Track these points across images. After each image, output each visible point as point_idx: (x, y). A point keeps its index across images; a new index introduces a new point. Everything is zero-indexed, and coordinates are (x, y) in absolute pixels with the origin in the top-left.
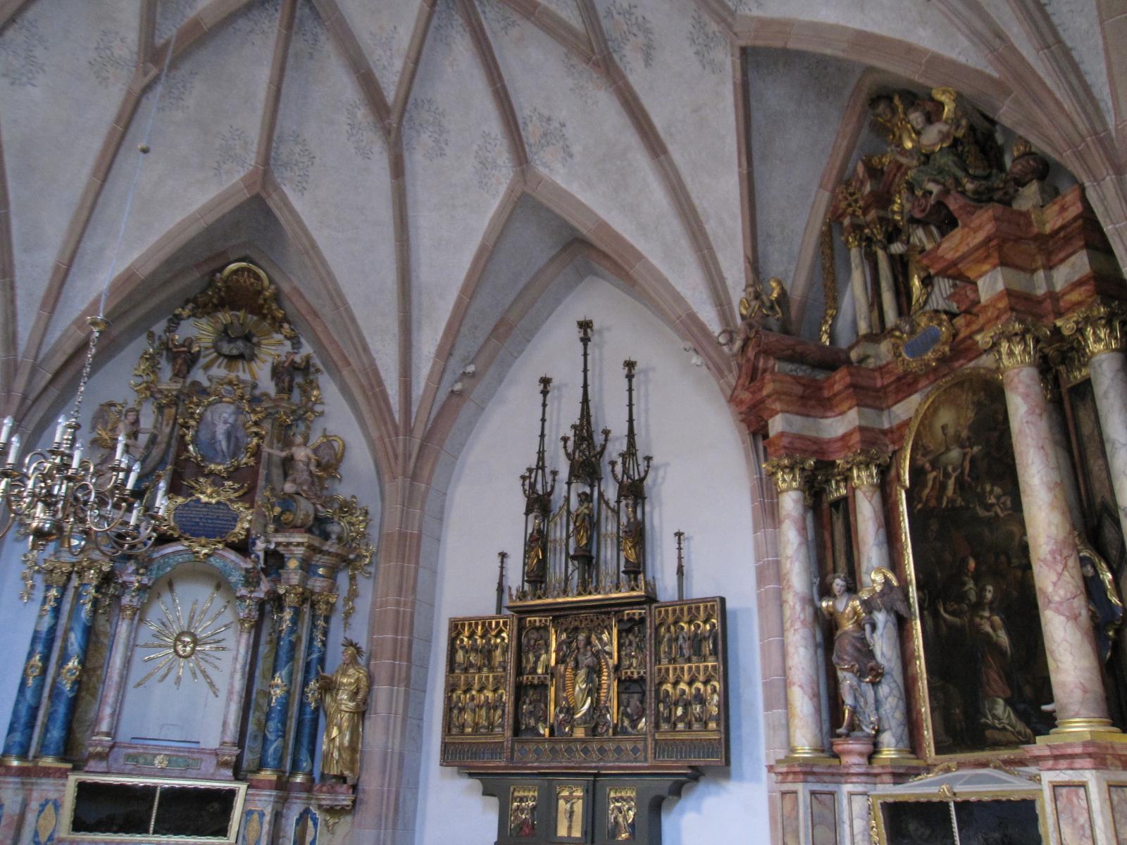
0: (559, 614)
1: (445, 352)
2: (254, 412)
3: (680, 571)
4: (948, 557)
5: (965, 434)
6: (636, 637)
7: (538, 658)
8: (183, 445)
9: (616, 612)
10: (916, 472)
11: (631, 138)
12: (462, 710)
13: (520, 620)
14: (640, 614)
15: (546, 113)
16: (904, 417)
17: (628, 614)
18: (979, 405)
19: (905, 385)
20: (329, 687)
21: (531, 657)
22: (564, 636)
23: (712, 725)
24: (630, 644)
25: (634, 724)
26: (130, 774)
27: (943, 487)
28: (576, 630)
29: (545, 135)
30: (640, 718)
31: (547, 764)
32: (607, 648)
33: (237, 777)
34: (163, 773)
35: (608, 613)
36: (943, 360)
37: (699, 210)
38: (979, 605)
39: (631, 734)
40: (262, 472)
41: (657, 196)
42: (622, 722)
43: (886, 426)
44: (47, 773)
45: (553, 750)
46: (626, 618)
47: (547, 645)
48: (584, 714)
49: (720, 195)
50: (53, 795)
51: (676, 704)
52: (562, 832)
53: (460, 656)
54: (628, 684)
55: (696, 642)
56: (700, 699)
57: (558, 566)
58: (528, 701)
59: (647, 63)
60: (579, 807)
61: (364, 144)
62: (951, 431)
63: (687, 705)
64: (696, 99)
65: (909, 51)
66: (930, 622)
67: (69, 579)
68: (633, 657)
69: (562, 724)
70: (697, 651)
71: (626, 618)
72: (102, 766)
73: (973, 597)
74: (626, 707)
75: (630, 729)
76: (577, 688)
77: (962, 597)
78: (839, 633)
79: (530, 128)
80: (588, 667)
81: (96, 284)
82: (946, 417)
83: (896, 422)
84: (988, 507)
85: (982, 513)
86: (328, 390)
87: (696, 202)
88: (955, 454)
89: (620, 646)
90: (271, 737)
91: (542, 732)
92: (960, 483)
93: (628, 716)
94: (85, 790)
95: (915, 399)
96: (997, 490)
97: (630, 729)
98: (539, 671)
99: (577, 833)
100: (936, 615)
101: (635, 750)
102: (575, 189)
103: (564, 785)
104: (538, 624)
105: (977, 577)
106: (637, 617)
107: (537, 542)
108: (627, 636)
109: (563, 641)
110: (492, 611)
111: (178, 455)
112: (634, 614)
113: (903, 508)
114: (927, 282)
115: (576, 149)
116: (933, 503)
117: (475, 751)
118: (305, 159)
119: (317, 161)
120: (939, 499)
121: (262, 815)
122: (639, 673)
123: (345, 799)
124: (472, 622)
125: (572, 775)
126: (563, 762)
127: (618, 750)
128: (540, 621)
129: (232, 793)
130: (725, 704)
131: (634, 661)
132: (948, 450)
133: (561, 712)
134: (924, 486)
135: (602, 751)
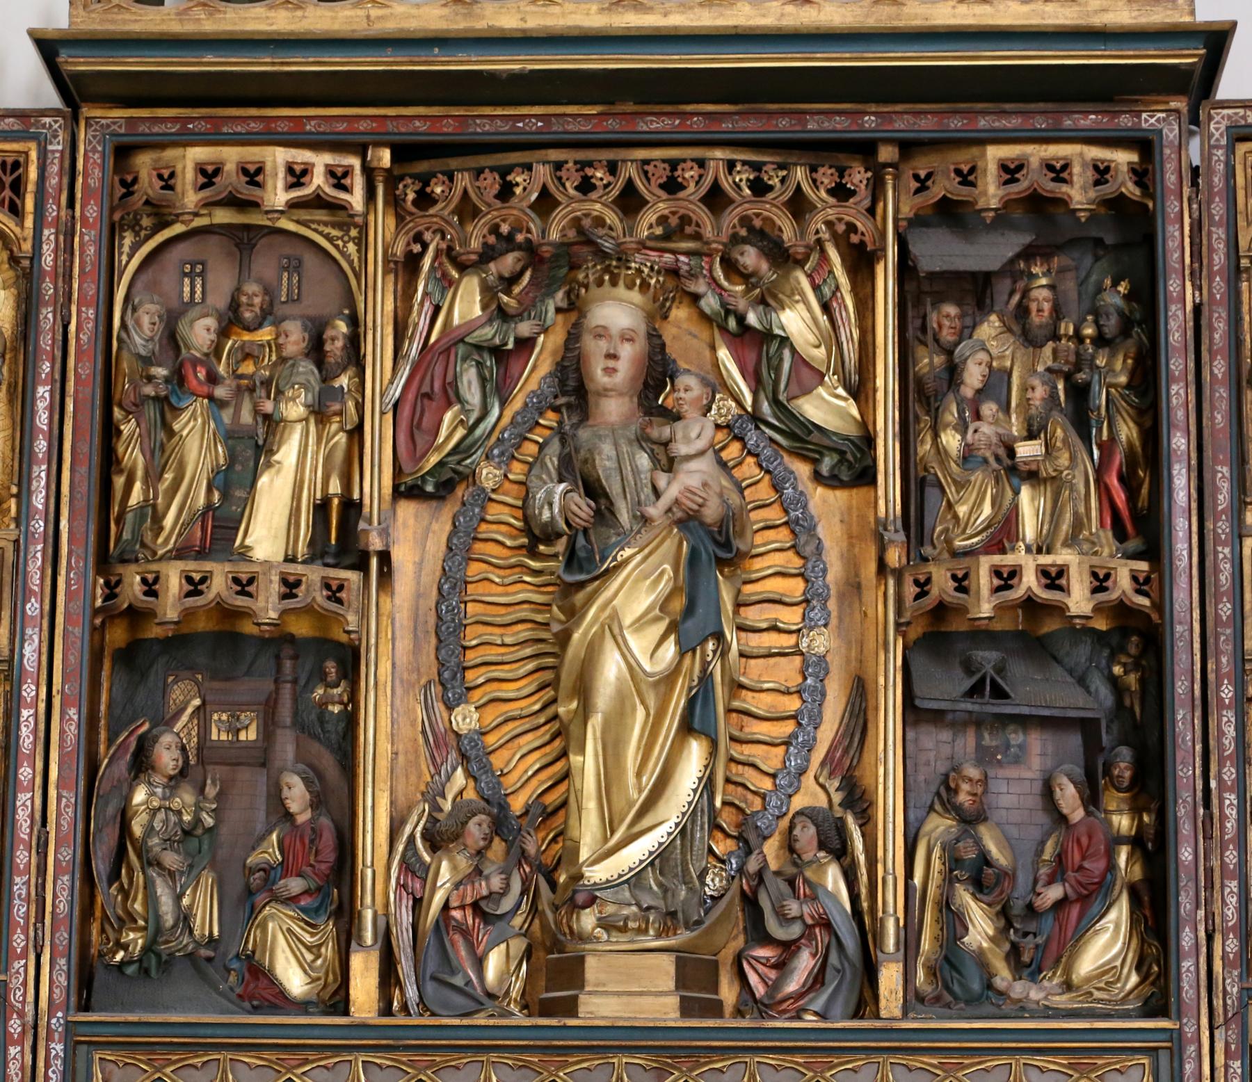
6: (1030, 339)
7: (249, 451)
9: (908, 147)
13: (123, 153)
14: (1102, 172)
17: (1011, 171)
21: (197, 442)
22: (467, 304)
24: (996, 384)
25: (1039, 940)
28: (565, 269)
30: (1088, 899)
32: (827, 407)
35: (865, 149)
39: (1022, 1009)
42: (953, 921)
46: (991, 193)
47: (333, 357)
48: (660, 858)
54: (987, 658)
58: (167, 757)
68: (1032, 477)
69: (441, 942)
71: (991, 193)
74: (970, 820)
75: (1003, 975)
76: (611, 668)
80: (687, 520)
89: (921, 400)
91: (294, 980)
93: (981, 877)
97: (1003, 975)
98: (268, 532)
104: (278, 195)
106: (1079, 194)
108: (966, 332)
109: (456, 341)
112: (1059, 172)
122: (1100, 582)
128: (297, 176)
131: (1030, 507)
133: (437, 840)
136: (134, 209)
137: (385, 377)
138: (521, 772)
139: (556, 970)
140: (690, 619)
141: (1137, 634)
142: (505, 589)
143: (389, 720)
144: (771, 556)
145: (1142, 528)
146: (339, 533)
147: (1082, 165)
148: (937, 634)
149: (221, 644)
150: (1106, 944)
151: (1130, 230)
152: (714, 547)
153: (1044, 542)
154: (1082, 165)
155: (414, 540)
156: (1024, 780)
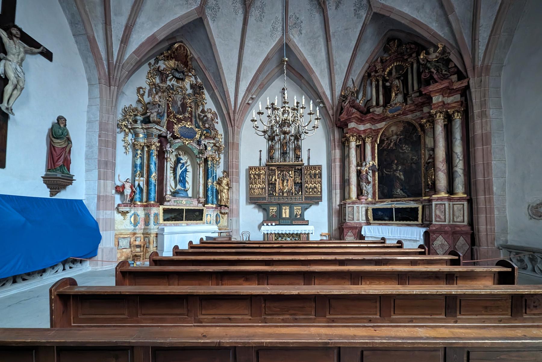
0: (279, 167)
1: (249, 90)
2: (190, 99)
3: (309, 158)
4: (388, 159)
5: (399, 133)
7: (272, 177)
8: (169, 107)
10: (382, 141)
11: (321, 33)
12: (254, 189)
15: (298, 16)
16: (379, 127)
18: (404, 127)
19: (383, 119)
20: (219, 183)
23: (319, 193)
25: (298, 193)
26: (176, 206)
27: (390, 144)
29: (295, 24)
31: (277, 201)
33: (204, 206)
34: (185, 205)
36: (399, 114)
37: (334, 61)
38: (397, 170)
40: (194, 120)
41: (323, 54)
43: (373, 128)
44: (153, 205)
45: (279, 199)
49: (342, 59)
50: (156, 212)
51: (310, 189)
52: (284, 216)
53: (252, 176)
55: (315, 175)
56: (315, 187)
57: (277, 155)
59: (336, 8)
60: (288, 211)
61: (236, 8)
62: (394, 132)
63: (312, 189)
64: (348, 25)
65: (427, 29)
66: (380, 174)
67: (143, 148)
70: (315, 177)
72: (168, 203)
73: (395, 168)
77: (392, 168)
78: (362, 174)
79: (291, 20)
81: (138, 38)
82: (393, 128)
83: (377, 128)
84: (403, 150)
85: (401, 151)
86: (207, 96)
87: (334, 59)
88: (395, 137)
89: (294, 175)
90: (210, 195)
92: (395, 144)
94: (165, 211)
95: (384, 123)
96: (406, 146)
99: (288, 216)
100: (382, 172)
101: (300, 198)
102: (299, 45)
103: (284, 206)
105: (396, 165)
107: (271, 149)
110: (258, 165)
111: (168, 110)
113: (376, 148)
114: (396, 95)
115: (303, 32)
116: (386, 148)
117: (258, 199)
118: (217, 8)
119: (220, 10)
120: (388, 147)
121: (211, 215)
123: (227, 211)
124: (255, 168)
125: (286, 204)
126: (282, 201)
127: (296, 198)
129: (203, 210)
130: (321, 189)
132: (393, 136)
134: (384, 143)
135: (291, 199)
136: (269, 169)
137: (277, 175)
138: (282, 188)
139: (283, 194)
140: (287, 183)
141: (301, 183)
142: (281, 182)
143: (277, 186)
144: (289, 181)
145: (301, 180)
146: (276, 180)
147: (300, 167)
148: (295, 183)
149: (272, 184)
150: (300, 193)
151: (301, 170)
152: (288, 180)
153: (298, 180)
154: (300, 167)
155: (278, 180)
156: (297, 188)
